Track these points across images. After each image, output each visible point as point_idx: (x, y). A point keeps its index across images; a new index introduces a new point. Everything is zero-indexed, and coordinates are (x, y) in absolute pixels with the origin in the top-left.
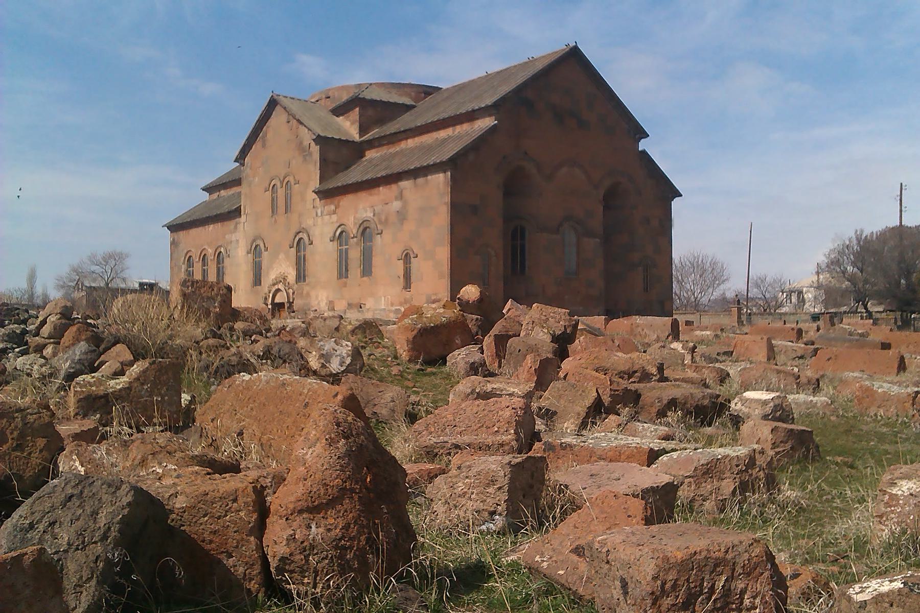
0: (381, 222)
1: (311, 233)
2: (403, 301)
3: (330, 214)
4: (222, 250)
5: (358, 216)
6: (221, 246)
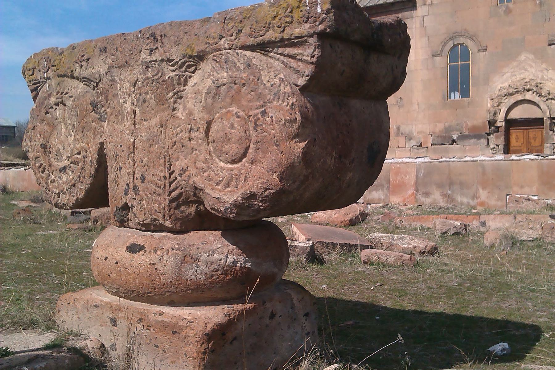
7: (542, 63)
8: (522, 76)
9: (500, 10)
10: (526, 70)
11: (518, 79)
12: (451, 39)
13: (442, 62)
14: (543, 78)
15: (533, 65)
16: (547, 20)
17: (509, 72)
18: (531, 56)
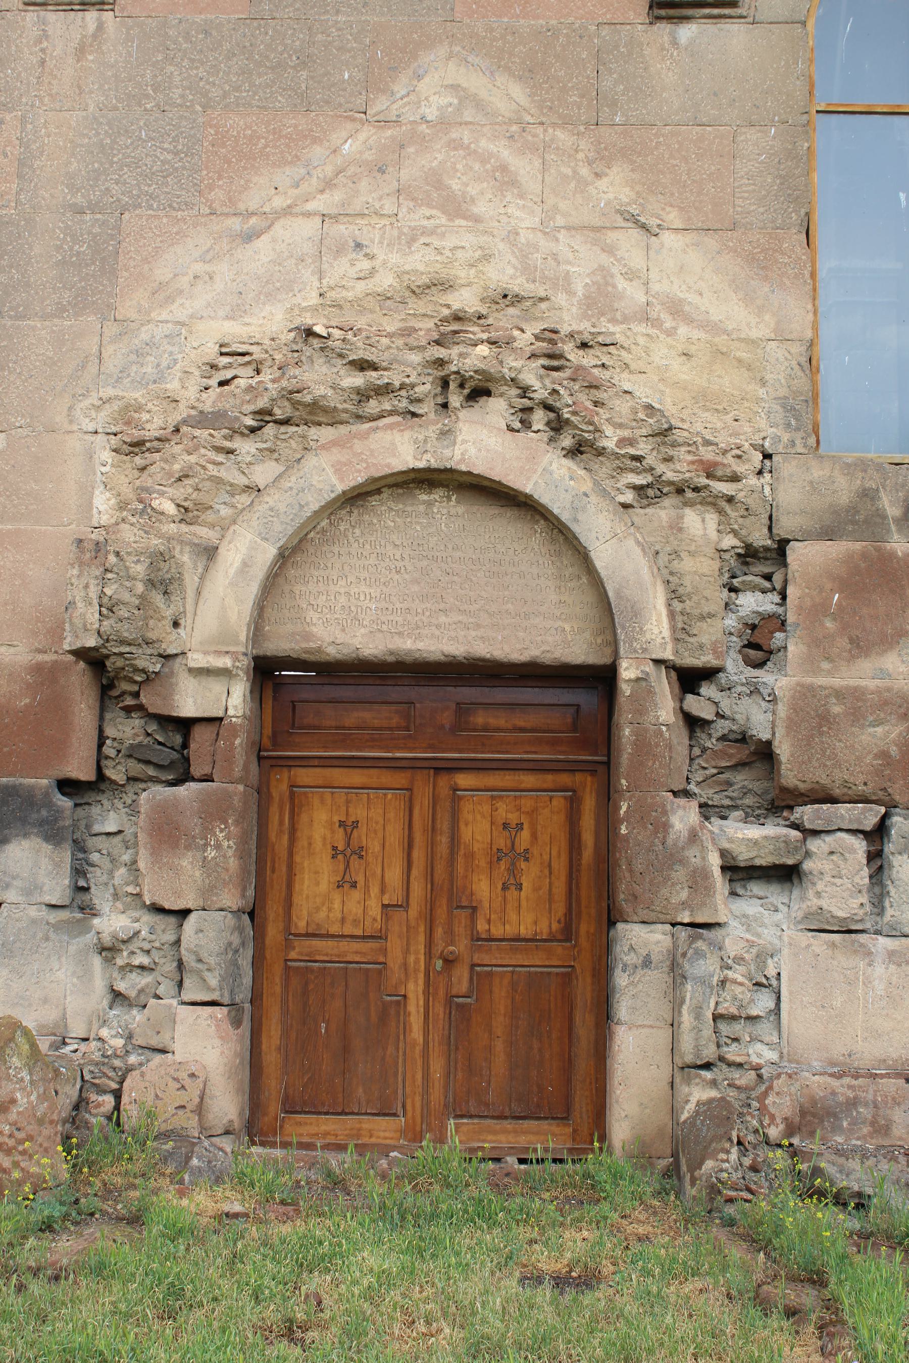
11: (385, 281)
17: (308, 215)
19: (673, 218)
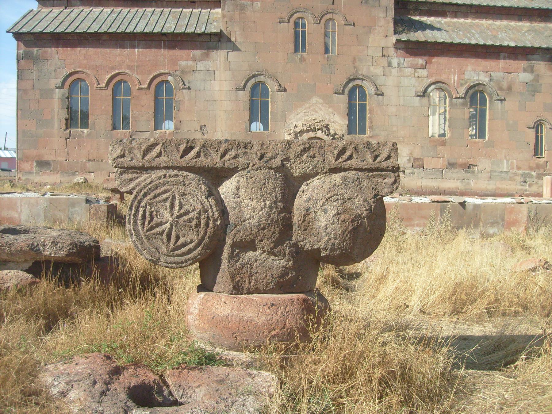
0: (501, 89)
1: (379, 82)
2: (534, 166)
3: (415, 67)
4: (170, 78)
5: (466, 77)
6: (169, 74)
7: (329, 107)
8: (313, 117)
9: (296, 58)
10: (316, 112)
11: (310, 119)
12: (254, 76)
13: (244, 95)
14: (329, 121)
15: (322, 108)
16: (333, 73)
18: (321, 101)
19: (336, 113)
